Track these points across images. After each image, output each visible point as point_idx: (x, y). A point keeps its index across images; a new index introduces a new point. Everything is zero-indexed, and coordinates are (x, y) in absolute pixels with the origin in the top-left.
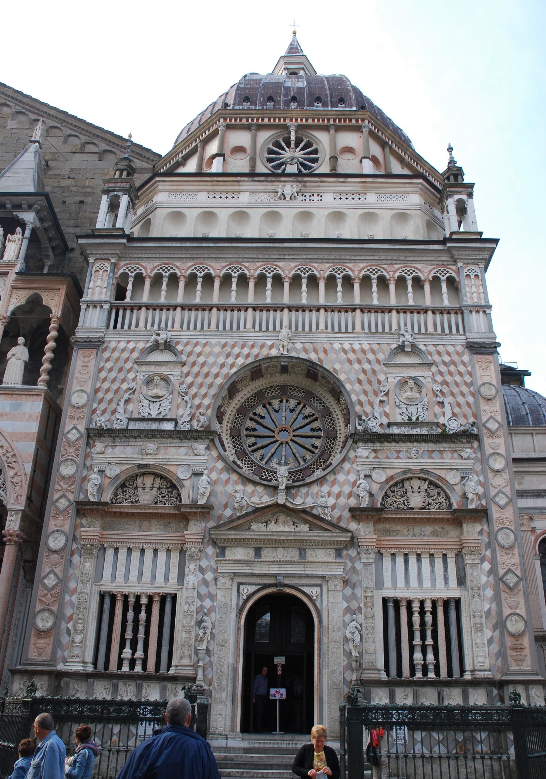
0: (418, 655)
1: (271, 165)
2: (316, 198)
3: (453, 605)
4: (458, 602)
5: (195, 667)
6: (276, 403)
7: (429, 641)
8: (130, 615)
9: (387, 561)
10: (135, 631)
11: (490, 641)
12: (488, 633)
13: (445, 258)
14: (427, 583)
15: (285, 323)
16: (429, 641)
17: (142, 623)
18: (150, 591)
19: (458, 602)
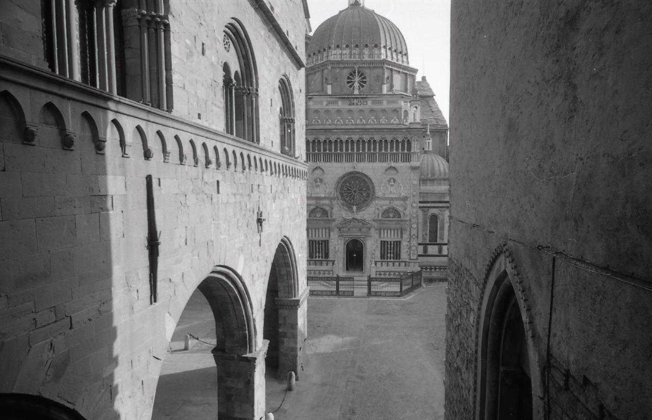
0: (389, 255)
1: (349, 85)
2: (365, 103)
3: (398, 243)
4: (400, 242)
5: (335, 258)
6: (353, 182)
7: (392, 251)
8: (317, 246)
9: (382, 231)
10: (319, 249)
11: (407, 252)
12: (407, 250)
13: (407, 133)
14: (392, 236)
15: (355, 159)
16: (392, 251)
17: (320, 248)
18: (322, 239)
19: (400, 242)
